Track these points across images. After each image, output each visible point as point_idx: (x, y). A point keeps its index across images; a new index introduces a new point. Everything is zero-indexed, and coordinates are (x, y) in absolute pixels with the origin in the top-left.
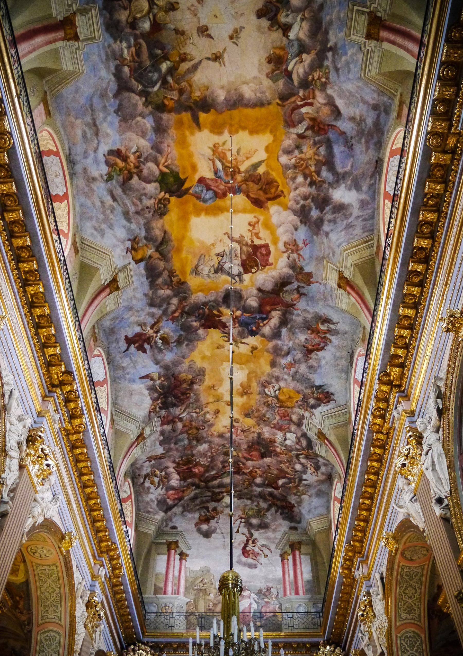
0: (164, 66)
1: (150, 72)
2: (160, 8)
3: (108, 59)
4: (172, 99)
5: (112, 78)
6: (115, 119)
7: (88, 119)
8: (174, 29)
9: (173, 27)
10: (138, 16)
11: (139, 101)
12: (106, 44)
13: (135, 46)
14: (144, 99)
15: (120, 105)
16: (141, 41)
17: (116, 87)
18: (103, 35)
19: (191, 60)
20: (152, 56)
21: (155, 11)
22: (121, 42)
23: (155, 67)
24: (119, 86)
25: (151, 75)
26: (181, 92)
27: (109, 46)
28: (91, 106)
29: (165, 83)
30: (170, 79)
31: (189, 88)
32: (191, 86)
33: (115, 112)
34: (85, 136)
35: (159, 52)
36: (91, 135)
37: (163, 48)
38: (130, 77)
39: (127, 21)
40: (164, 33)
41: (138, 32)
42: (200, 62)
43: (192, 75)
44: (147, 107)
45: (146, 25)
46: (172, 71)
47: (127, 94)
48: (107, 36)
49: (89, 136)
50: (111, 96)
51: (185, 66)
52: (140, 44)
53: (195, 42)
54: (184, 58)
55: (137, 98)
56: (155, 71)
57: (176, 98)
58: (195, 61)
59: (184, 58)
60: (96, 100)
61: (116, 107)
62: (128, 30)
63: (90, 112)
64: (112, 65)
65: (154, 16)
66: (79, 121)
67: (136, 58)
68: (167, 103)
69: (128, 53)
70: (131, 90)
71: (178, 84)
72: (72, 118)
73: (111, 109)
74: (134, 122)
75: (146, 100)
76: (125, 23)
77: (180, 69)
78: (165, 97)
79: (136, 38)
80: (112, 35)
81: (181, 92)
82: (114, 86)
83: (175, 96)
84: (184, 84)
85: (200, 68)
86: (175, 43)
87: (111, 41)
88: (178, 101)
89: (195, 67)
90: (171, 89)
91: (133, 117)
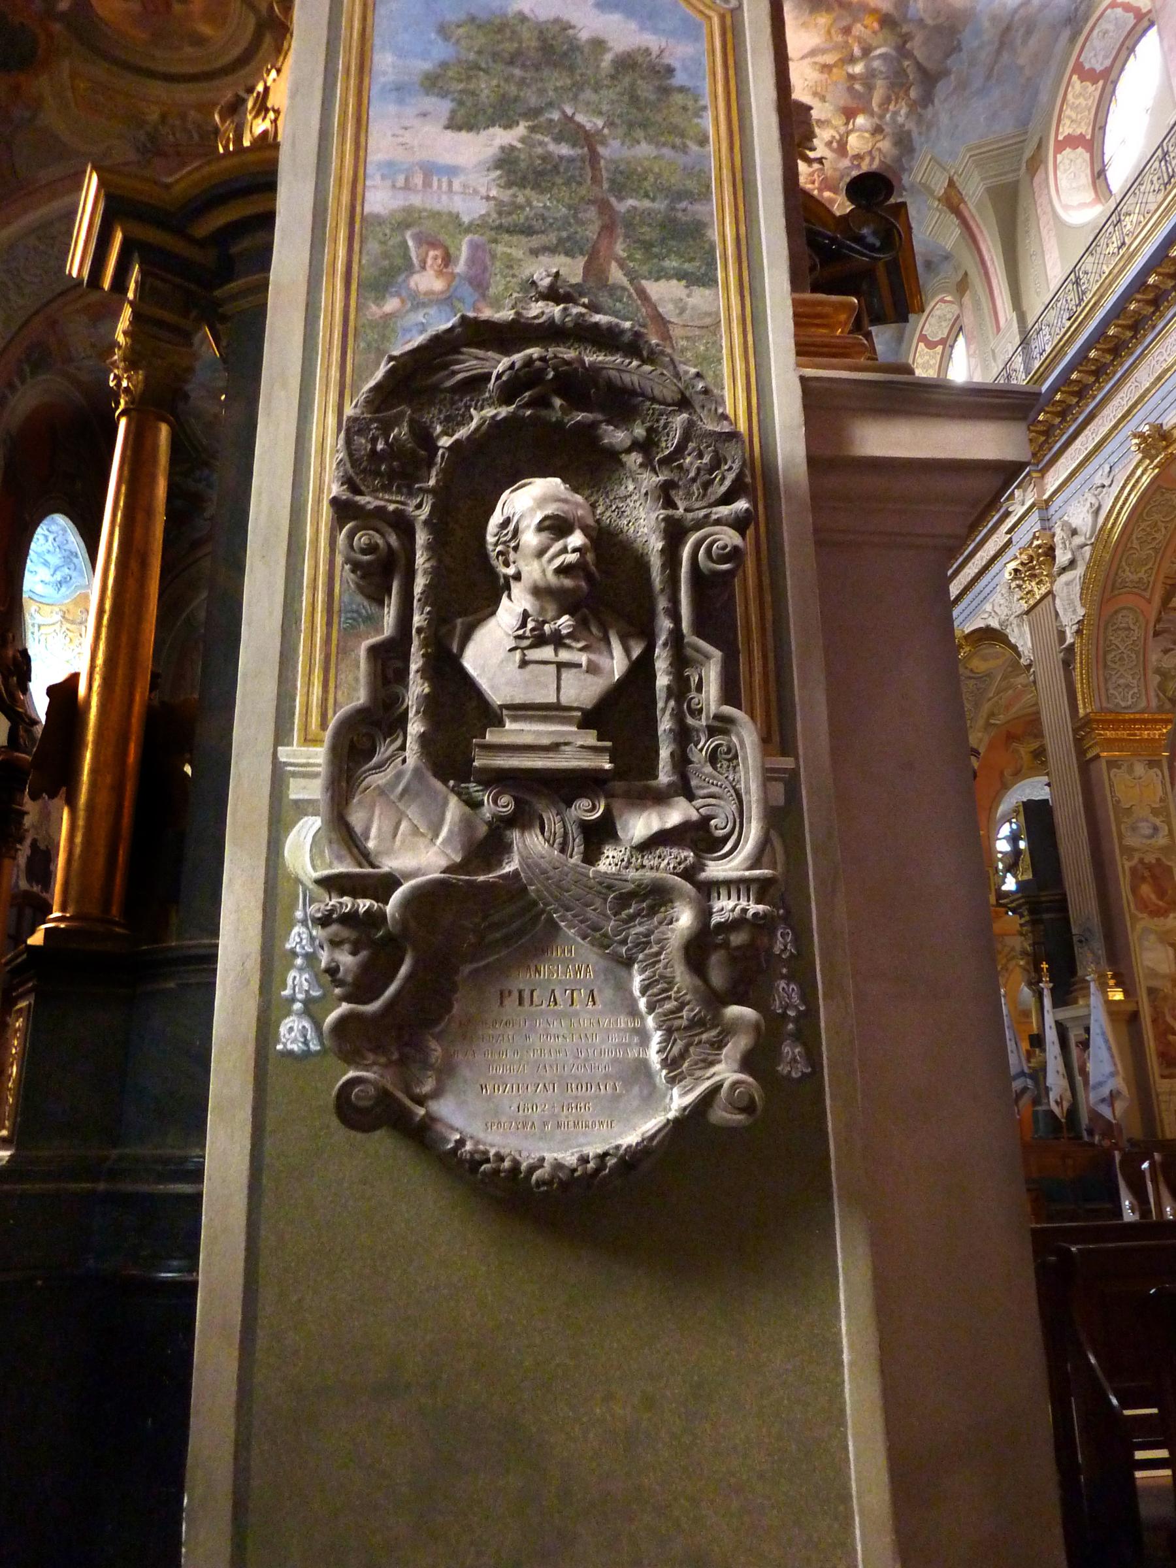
0: (858, 69)
1: (881, 72)
2: (835, 128)
3: (929, 127)
4: (866, 27)
5: (936, 101)
6: (969, 41)
7: (1006, 57)
8: (825, 102)
9: (827, 104)
10: (867, 135)
11: (916, 46)
12: (923, 139)
13: (887, 110)
14: (908, 46)
15: (947, 55)
16: (876, 109)
17: (939, 85)
18: (921, 150)
19: (816, 63)
20: (870, 88)
21: (842, 129)
22: (903, 126)
23: (870, 75)
24: (934, 86)
25: (883, 69)
26: (847, 31)
27: (920, 134)
28: (988, 77)
29: (866, 51)
30: (857, 51)
31: (833, 31)
32: (829, 32)
33: (960, 50)
34: (1029, 32)
35: (858, 87)
36: (1017, 31)
37: (850, 89)
38: (912, 84)
39: (884, 138)
40: (842, 103)
41: (876, 120)
42: (803, 58)
43: (822, 46)
44: (907, 34)
45: (861, 120)
46: (852, 60)
47: (928, 65)
48: (917, 145)
49: (1022, 31)
50: (953, 77)
51: (829, 59)
52: (880, 106)
53: (801, 81)
54: (826, 68)
55: (916, 53)
56: (874, 70)
57: (859, 25)
58: (808, 60)
59: (826, 68)
60: (977, 83)
61: (954, 56)
62: (887, 130)
63: (996, 68)
64: (929, 112)
65: (847, 124)
66: (1022, 61)
67: (893, 98)
68: (876, 25)
69: (901, 108)
70: (920, 68)
71: (847, 42)
72: (1027, 72)
73: (964, 55)
74: (940, 21)
75: (905, 42)
76: (888, 138)
77: (836, 58)
78: (875, 33)
79: (882, 117)
80: (911, 141)
81: (847, 31)
82: (942, 89)
83: (858, 29)
84: (839, 38)
85: (806, 51)
86: (830, 88)
87: (915, 135)
88: (856, 20)
89: (813, 53)
90: (859, 40)
91: (938, 29)
